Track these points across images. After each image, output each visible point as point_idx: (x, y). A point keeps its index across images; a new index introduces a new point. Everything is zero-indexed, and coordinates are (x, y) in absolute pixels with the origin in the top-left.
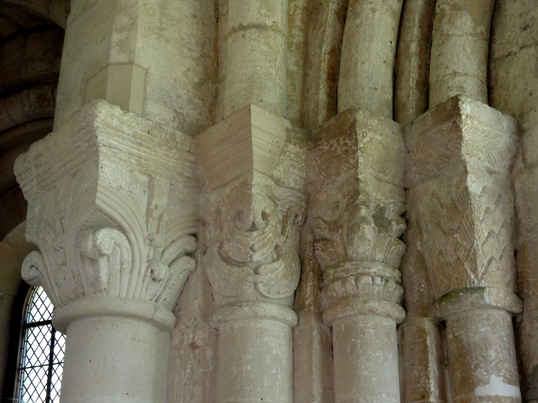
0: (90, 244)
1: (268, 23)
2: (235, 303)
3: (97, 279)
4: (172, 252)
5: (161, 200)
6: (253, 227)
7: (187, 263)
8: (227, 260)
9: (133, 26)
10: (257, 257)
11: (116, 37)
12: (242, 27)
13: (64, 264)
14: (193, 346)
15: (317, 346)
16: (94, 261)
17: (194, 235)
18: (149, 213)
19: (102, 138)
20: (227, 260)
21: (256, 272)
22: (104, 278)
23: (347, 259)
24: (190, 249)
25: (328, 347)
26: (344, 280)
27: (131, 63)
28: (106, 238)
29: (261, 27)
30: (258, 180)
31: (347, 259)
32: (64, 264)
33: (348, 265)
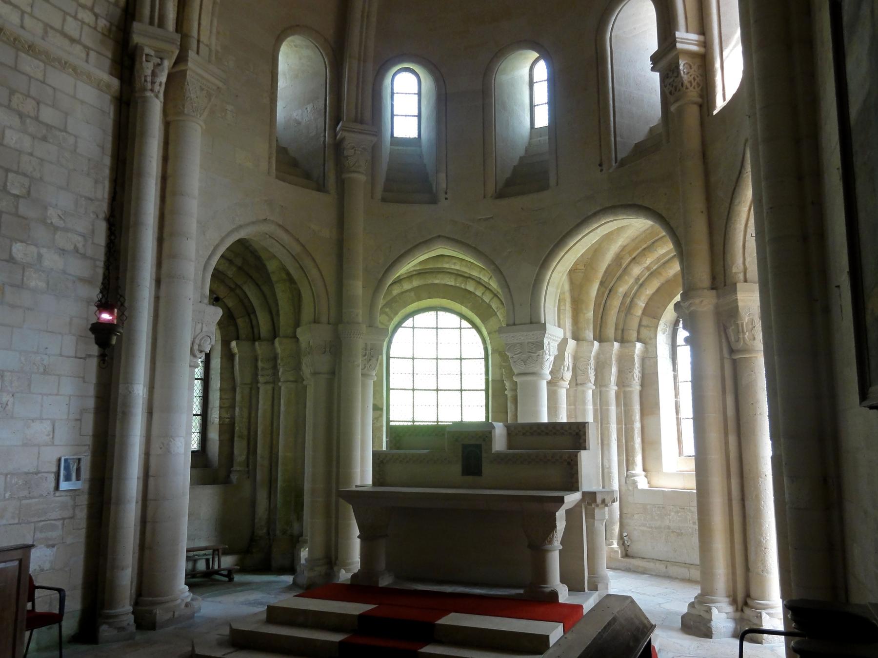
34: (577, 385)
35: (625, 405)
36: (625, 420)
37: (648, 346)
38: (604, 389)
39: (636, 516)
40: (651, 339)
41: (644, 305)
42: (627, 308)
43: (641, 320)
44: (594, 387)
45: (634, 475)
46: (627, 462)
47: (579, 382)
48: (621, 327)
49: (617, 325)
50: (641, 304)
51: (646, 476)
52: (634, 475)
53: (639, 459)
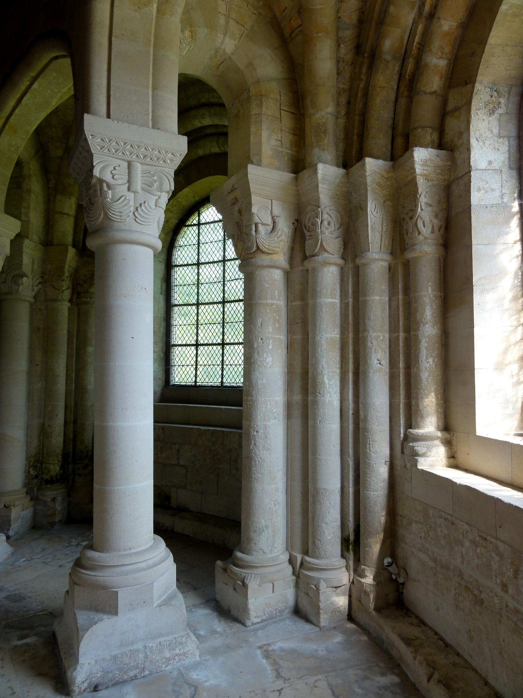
0: (21, 282)
1: (71, 214)
2: (55, 300)
3: (18, 290)
4: (37, 283)
5: (35, 267)
6: (63, 280)
7: (40, 286)
8: (53, 287)
9: (28, 208)
10: (64, 288)
11: (23, 210)
12: (62, 213)
13: (5, 282)
14: (40, 309)
15: (76, 314)
16: (19, 286)
17: (41, 277)
18: (32, 271)
19: (24, 249)
20: (53, 287)
21: (63, 292)
22: (20, 290)
23: (88, 292)
24: (41, 281)
25: (79, 314)
26: (87, 298)
27: (28, 221)
28: (25, 279)
29: (68, 215)
30: (66, 266)
31: (88, 292)
32: (5, 282)
33: (88, 294)
34: (305, 258)
35: (407, 290)
36: (405, 322)
37: (457, 154)
38: (358, 261)
39: (414, 526)
40: (461, 134)
41: (442, 63)
42: (409, 85)
43: (445, 102)
44: (340, 262)
45: (418, 439)
46: (406, 412)
47: (308, 255)
48: (400, 129)
49: (394, 128)
50: (437, 61)
51: (448, 443)
52: (418, 439)
53: (430, 402)
